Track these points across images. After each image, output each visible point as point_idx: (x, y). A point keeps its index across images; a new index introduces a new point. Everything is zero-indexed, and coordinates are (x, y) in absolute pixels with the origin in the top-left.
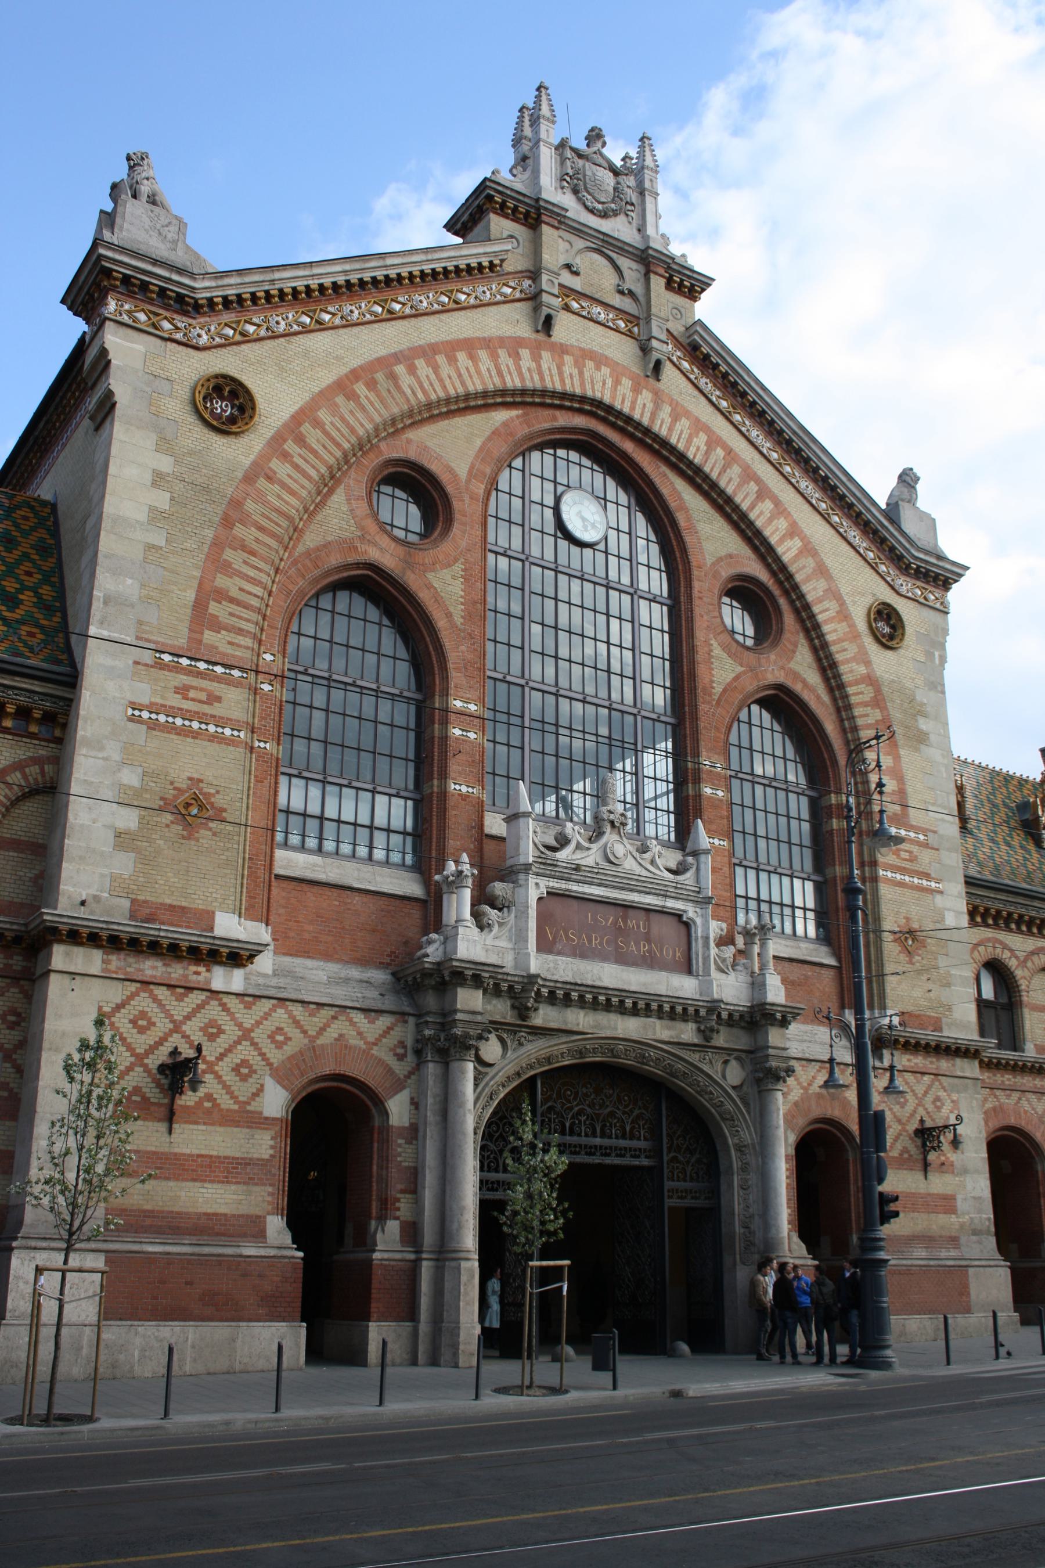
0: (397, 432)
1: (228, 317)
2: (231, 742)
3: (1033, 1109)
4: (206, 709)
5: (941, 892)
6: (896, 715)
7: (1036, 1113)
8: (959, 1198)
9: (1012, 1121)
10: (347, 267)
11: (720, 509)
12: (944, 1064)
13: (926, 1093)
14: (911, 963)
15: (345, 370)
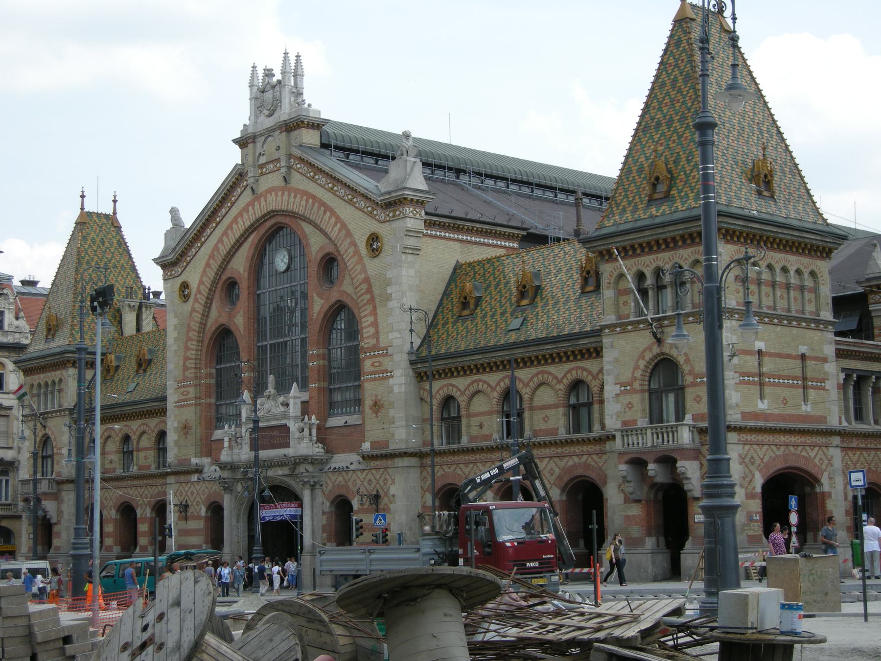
0: (224, 269)
1: (184, 259)
2: (190, 405)
3: (463, 472)
4: (187, 397)
5: (392, 376)
6: (376, 291)
9: (451, 481)
12: (389, 462)
14: (377, 417)
15: (207, 257)
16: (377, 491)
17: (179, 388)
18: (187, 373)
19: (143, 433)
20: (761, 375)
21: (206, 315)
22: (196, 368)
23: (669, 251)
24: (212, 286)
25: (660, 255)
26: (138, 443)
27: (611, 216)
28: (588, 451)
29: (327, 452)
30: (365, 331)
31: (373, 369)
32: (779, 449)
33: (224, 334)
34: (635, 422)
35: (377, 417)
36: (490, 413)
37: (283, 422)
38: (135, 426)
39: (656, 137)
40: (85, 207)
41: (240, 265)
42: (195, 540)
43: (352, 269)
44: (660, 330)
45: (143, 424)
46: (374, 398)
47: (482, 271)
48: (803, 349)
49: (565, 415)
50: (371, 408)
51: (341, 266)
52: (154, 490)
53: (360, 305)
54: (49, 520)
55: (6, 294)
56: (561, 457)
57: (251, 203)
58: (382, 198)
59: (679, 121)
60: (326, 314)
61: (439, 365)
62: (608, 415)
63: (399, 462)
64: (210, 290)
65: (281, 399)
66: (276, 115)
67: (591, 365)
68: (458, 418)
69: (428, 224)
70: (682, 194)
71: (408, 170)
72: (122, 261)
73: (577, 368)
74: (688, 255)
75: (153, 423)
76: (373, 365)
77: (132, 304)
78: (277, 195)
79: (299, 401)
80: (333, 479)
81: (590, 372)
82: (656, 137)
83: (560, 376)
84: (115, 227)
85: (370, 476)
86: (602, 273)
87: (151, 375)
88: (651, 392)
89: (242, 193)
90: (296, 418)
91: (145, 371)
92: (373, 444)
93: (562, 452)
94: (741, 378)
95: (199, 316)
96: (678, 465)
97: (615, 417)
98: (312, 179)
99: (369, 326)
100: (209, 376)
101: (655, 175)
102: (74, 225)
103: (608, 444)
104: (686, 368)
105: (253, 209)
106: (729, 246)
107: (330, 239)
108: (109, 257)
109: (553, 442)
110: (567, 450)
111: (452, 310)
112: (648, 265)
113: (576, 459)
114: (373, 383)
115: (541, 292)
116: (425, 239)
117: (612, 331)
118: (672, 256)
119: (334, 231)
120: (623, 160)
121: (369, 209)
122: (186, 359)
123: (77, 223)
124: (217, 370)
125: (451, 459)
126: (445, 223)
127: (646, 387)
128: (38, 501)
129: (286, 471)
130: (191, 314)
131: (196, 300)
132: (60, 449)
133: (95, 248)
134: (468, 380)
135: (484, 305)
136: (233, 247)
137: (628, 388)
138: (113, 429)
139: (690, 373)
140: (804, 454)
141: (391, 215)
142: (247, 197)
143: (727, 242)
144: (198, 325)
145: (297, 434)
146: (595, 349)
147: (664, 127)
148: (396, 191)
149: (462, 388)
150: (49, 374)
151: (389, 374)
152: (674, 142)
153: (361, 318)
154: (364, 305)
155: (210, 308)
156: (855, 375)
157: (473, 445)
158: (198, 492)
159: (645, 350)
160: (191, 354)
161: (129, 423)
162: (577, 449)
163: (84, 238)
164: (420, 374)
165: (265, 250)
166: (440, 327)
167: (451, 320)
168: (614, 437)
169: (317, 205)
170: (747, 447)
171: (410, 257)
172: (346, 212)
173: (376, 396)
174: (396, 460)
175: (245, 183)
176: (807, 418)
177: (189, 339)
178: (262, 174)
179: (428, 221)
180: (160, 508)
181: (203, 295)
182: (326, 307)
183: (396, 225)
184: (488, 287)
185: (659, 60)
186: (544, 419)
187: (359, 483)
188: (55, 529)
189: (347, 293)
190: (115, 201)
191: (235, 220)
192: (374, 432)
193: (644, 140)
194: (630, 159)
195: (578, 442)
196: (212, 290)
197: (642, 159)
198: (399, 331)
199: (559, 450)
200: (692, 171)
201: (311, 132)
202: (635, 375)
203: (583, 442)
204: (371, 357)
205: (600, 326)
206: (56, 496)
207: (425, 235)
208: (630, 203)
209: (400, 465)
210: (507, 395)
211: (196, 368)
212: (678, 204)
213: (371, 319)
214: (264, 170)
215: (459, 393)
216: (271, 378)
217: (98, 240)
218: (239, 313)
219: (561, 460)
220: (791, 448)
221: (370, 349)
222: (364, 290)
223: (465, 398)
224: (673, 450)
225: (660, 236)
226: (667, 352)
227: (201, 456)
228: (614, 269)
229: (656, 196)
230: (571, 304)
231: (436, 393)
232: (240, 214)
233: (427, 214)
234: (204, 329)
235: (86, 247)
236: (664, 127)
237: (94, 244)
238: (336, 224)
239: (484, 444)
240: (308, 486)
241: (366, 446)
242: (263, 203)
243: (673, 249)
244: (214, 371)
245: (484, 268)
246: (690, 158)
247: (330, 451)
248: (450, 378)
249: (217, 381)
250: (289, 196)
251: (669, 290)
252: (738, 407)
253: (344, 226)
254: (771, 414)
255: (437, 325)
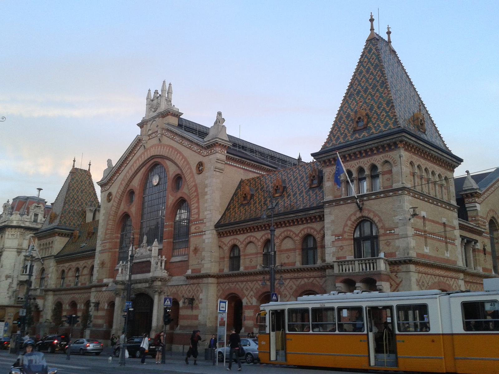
0: (129, 185)
1: (111, 182)
5: (205, 234)
6: (199, 191)
7: (241, 288)
8: (199, 316)
9: (233, 291)
10: (119, 162)
11: (173, 162)
12: (200, 280)
13: (195, 289)
14: (196, 256)
16: (193, 296)
17: (102, 243)
18: (106, 236)
19: (85, 267)
20: (425, 231)
21: (118, 208)
22: (110, 234)
23: (367, 157)
24: (122, 193)
25: (361, 160)
26: (82, 272)
27: (330, 142)
28: (313, 275)
29: (170, 275)
30: (192, 211)
31: (195, 231)
32: (435, 278)
33: (126, 216)
34: (345, 257)
35: (196, 256)
36: (257, 254)
37: (148, 259)
38: (81, 264)
39: (358, 99)
40: (75, 166)
41: (136, 184)
42: (100, 321)
43: (188, 181)
44: (361, 203)
45: (86, 262)
46: (195, 246)
47: (254, 183)
48: (444, 220)
49: (299, 254)
50: (193, 251)
51: (183, 179)
52: (86, 296)
53: (191, 198)
54: (39, 309)
55: (40, 207)
56: (296, 278)
57: (143, 153)
58: (205, 143)
59: (372, 88)
60: (174, 205)
61: (230, 228)
62: (327, 253)
63: (205, 280)
64: (121, 196)
65: (149, 247)
66: (158, 111)
67: (316, 226)
68: (239, 257)
69: (228, 158)
70: (376, 125)
71: (220, 130)
72: (90, 191)
73: (308, 228)
74: (380, 158)
75: (89, 262)
76: (195, 229)
77: (92, 209)
78: (155, 149)
79: (157, 249)
80: (171, 290)
81: (315, 230)
82: (358, 99)
83: (297, 232)
84: (88, 176)
85: (190, 288)
86: (324, 173)
87: (92, 239)
88: (355, 240)
89: (139, 148)
90: (155, 257)
91: (90, 237)
92: (193, 271)
93: (298, 276)
94: (415, 232)
95: (115, 208)
96: (377, 284)
97: (332, 255)
98: (172, 139)
99: (195, 209)
100: (117, 237)
101: (358, 116)
102: (69, 173)
103: (327, 271)
104: (380, 225)
105: (144, 156)
106: (407, 153)
107: (178, 167)
108: (84, 188)
109: (292, 270)
110: (301, 275)
111: (238, 201)
112: (353, 167)
113: (305, 280)
114: (195, 238)
115: (286, 190)
116: (226, 166)
117: (330, 205)
118: (370, 160)
119: (181, 163)
120: (337, 112)
121: (199, 150)
122: (107, 229)
123: (70, 172)
124: (121, 235)
125: (234, 279)
126: (236, 159)
127: (352, 237)
128: (34, 299)
129: (147, 285)
130: (111, 208)
131: (114, 201)
132: (48, 274)
133: (77, 184)
134: (244, 236)
135: (255, 198)
136: (133, 174)
137: (340, 237)
138: (71, 265)
139: (382, 228)
140: (448, 282)
141: (209, 152)
142: (142, 150)
143: (406, 150)
144: (114, 212)
145: (155, 265)
146: (319, 216)
147: (362, 93)
148: (212, 139)
149: (241, 240)
150: (48, 239)
151: (203, 233)
152: (369, 99)
153: (191, 205)
154: (193, 198)
155: (120, 204)
156: (466, 240)
157: (247, 271)
158: (105, 296)
159: (351, 215)
160: (109, 227)
161: (79, 262)
162: (307, 274)
163: (73, 179)
164: (219, 233)
165: (148, 176)
166: (231, 210)
167: (237, 206)
168: (332, 267)
169: (174, 151)
170: (420, 275)
171: (218, 173)
172: (187, 153)
173: (196, 245)
174: (204, 279)
175: (141, 144)
176: (448, 260)
177: (109, 220)
178: (149, 139)
179: (228, 157)
180: (88, 304)
181: (118, 198)
182: (175, 200)
183: (212, 157)
184: (258, 189)
185: (358, 61)
186: (287, 257)
187: (184, 292)
188: (42, 313)
189: (185, 193)
190: (90, 165)
191: (135, 162)
192: (193, 262)
193: (350, 101)
194: (341, 112)
195: (308, 270)
196: (122, 196)
197: (349, 110)
198: (210, 210)
199: (296, 275)
200: (381, 112)
201: (174, 118)
202: (345, 230)
203: (311, 270)
204: (195, 224)
205: (323, 202)
206: (44, 298)
207: (226, 164)
208: (342, 134)
209: (206, 282)
210: (268, 243)
211: (110, 234)
212: (373, 130)
213: (196, 205)
214: (151, 137)
215: (239, 243)
216: (145, 238)
217: (79, 180)
218: (133, 206)
219: (297, 281)
220: (441, 278)
221: (194, 221)
222: (194, 191)
223: (243, 246)
224: (374, 274)
225: (362, 148)
226: (366, 215)
227: (109, 278)
228: (332, 170)
229: (358, 128)
230: (304, 194)
231: (228, 243)
232: (138, 159)
233: (227, 153)
234: (117, 215)
235: (73, 183)
236: (362, 93)
237: (77, 182)
238: (182, 159)
239: (253, 270)
240: (157, 293)
241: (189, 272)
242: (149, 152)
243: (370, 156)
244: (119, 235)
245: (255, 181)
246: (380, 106)
247: (171, 275)
248: (235, 235)
249: (121, 240)
250: (161, 148)
251: (367, 179)
252: (414, 249)
253: (186, 160)
254: (431, 256)
255: (230, 209)
